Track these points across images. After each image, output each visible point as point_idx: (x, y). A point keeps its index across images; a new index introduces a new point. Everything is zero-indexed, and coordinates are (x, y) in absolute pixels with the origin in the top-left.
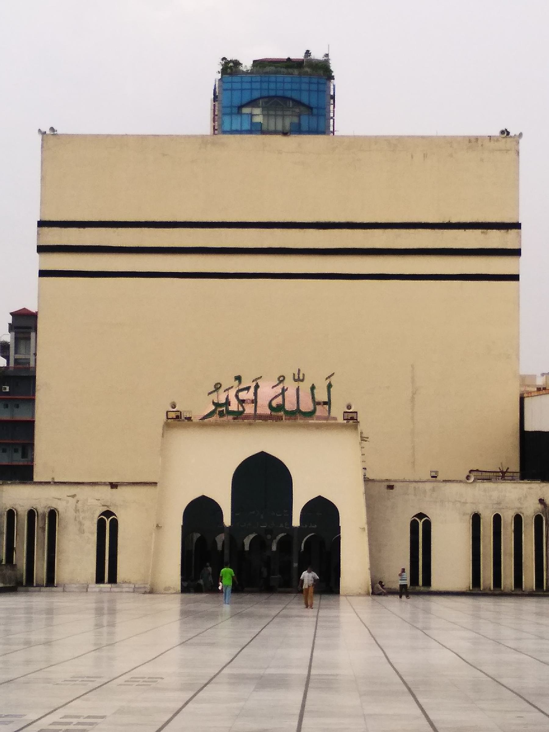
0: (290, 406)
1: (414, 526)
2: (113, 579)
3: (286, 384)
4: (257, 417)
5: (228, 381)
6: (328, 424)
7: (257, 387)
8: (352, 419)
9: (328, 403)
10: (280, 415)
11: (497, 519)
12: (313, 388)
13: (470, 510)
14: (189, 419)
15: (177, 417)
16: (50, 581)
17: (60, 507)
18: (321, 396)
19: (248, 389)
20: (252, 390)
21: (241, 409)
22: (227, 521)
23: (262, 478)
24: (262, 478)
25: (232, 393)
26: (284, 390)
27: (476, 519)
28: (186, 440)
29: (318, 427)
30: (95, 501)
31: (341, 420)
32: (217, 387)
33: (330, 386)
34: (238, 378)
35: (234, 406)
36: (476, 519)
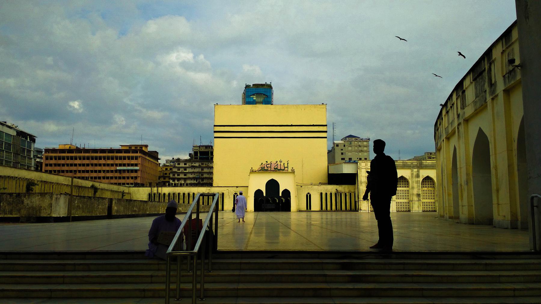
1: (307, 195)
4: (271, 170)
6: (288, 172)
8: (293, 172)
9: (287, 167)
11: (326, 194)
13: (320, 192)
16: (223, 209)
17: (225, 192)
18: (286, 166)
22: (265, 195)
23: (272, 185)
24: (272, 185)
27: (321, 194)
30: (233, 191)
32: (262, 164)
35: (266, 168)
36: (321, 194)
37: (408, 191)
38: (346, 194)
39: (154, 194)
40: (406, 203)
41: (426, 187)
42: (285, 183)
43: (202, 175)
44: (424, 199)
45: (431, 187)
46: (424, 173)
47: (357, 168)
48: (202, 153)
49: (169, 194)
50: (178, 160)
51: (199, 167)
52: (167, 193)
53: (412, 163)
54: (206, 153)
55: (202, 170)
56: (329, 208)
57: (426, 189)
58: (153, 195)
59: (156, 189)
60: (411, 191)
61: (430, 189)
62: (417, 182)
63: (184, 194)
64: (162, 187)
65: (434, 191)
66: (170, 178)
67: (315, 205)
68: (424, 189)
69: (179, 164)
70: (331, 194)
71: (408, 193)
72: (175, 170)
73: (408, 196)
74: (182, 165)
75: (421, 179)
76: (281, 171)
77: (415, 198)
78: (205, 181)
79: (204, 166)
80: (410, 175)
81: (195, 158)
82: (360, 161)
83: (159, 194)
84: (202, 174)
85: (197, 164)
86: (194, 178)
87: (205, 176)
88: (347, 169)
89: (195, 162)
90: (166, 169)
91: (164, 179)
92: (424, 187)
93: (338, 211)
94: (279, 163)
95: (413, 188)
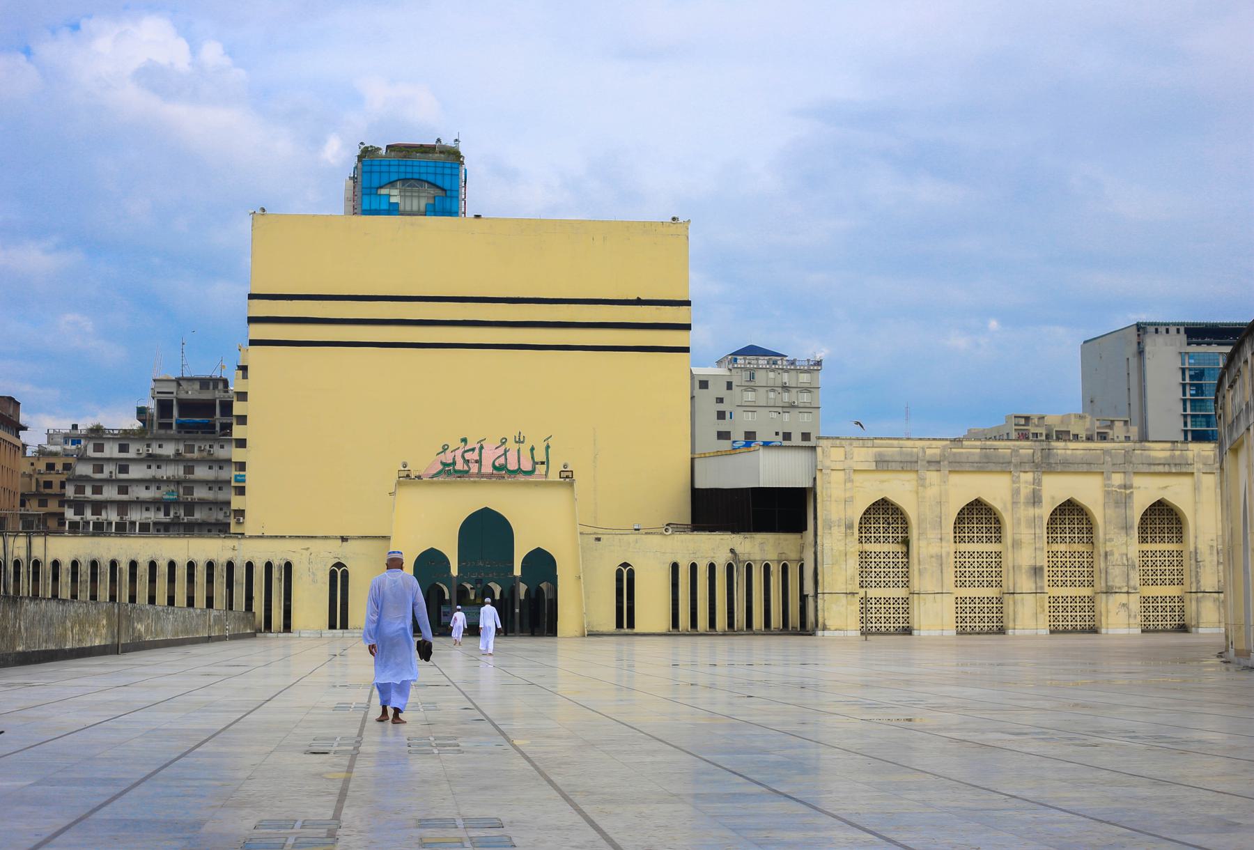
0: (512, 465)
2: (344, 626)
3: (508, 445)
4: (480, 474)
5: (455, 443)
7: (482, 448)
8: (567, 477)
10: (502, 472)
12: (532, 449)
14: (419, 477)
15: (408, 476)
18: (540, 456)
19: (473, 450)
20: (477, 451)
21: (466, 468)
22: (454, 571)
23: (486, 532)
24: (486, 532)
25: (459, 453)
26: (505, 454)
28: (413, 497)
29: (537, 484)
30: (328, 553)
31: (558, 479)
33: (548, 447)
34: (464, 440)
35: (460, 466)
37: (999, 554)
38: (767, 567)
39: (17, 564)
40: (990, 600)
41: (1063, 540)
42: (536, 522)
43: (189, 491)
44: (1055, 584)
45: (1081, 539)
46: (1057, 489)
47: (815, 469)
48: (188, 407)
49: (75, 564)
50: (97, 433)
51: (177, 459)
52: (66, 563)
53: (1015, 451)
54: (206, 407)
55: (189, 470)
56: (703, 622)
57: (1062, 547)
58: (11, 568)
59: (21, 542)
60: (1008, 560)
61: (1078, 547)
62: (1033, 522)
63: (133, 565)
64: (47, 533)
65: (1091, 555)
66: (63, 502)
67: (652, 606)
68: (1055, 547)
69: (99, 448)
70: (712, 567)
71: (999, 564)
72: (84, 469)
73: (999, 574)
74: (111, 450)
75: (1046, 511)
76: (522, 478)
77: (1026, 584)
78: (198, 515)
79: (196, 455)
80: (1008, 497)
81: (162, 426)
82: (823, 443)
83: (37, 563)
84: (188, 485)
85: (169, 450)
86: (156, 504)
87: (200, 493)
88: (774, 470)
89: (161, 440)
90: (50, 467)
91: (43, 503)
92: (1054, 540)
93: (739, 633)
94: (511, 445)
95: (1016, 544)
